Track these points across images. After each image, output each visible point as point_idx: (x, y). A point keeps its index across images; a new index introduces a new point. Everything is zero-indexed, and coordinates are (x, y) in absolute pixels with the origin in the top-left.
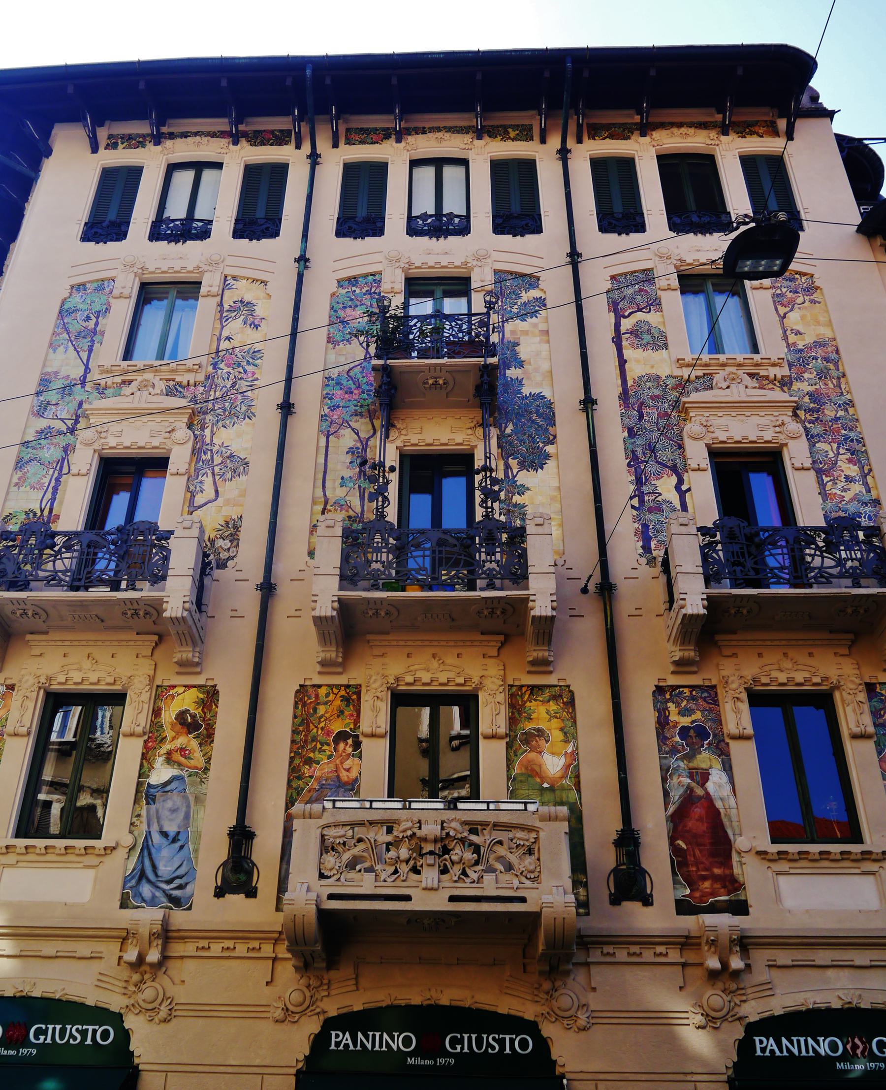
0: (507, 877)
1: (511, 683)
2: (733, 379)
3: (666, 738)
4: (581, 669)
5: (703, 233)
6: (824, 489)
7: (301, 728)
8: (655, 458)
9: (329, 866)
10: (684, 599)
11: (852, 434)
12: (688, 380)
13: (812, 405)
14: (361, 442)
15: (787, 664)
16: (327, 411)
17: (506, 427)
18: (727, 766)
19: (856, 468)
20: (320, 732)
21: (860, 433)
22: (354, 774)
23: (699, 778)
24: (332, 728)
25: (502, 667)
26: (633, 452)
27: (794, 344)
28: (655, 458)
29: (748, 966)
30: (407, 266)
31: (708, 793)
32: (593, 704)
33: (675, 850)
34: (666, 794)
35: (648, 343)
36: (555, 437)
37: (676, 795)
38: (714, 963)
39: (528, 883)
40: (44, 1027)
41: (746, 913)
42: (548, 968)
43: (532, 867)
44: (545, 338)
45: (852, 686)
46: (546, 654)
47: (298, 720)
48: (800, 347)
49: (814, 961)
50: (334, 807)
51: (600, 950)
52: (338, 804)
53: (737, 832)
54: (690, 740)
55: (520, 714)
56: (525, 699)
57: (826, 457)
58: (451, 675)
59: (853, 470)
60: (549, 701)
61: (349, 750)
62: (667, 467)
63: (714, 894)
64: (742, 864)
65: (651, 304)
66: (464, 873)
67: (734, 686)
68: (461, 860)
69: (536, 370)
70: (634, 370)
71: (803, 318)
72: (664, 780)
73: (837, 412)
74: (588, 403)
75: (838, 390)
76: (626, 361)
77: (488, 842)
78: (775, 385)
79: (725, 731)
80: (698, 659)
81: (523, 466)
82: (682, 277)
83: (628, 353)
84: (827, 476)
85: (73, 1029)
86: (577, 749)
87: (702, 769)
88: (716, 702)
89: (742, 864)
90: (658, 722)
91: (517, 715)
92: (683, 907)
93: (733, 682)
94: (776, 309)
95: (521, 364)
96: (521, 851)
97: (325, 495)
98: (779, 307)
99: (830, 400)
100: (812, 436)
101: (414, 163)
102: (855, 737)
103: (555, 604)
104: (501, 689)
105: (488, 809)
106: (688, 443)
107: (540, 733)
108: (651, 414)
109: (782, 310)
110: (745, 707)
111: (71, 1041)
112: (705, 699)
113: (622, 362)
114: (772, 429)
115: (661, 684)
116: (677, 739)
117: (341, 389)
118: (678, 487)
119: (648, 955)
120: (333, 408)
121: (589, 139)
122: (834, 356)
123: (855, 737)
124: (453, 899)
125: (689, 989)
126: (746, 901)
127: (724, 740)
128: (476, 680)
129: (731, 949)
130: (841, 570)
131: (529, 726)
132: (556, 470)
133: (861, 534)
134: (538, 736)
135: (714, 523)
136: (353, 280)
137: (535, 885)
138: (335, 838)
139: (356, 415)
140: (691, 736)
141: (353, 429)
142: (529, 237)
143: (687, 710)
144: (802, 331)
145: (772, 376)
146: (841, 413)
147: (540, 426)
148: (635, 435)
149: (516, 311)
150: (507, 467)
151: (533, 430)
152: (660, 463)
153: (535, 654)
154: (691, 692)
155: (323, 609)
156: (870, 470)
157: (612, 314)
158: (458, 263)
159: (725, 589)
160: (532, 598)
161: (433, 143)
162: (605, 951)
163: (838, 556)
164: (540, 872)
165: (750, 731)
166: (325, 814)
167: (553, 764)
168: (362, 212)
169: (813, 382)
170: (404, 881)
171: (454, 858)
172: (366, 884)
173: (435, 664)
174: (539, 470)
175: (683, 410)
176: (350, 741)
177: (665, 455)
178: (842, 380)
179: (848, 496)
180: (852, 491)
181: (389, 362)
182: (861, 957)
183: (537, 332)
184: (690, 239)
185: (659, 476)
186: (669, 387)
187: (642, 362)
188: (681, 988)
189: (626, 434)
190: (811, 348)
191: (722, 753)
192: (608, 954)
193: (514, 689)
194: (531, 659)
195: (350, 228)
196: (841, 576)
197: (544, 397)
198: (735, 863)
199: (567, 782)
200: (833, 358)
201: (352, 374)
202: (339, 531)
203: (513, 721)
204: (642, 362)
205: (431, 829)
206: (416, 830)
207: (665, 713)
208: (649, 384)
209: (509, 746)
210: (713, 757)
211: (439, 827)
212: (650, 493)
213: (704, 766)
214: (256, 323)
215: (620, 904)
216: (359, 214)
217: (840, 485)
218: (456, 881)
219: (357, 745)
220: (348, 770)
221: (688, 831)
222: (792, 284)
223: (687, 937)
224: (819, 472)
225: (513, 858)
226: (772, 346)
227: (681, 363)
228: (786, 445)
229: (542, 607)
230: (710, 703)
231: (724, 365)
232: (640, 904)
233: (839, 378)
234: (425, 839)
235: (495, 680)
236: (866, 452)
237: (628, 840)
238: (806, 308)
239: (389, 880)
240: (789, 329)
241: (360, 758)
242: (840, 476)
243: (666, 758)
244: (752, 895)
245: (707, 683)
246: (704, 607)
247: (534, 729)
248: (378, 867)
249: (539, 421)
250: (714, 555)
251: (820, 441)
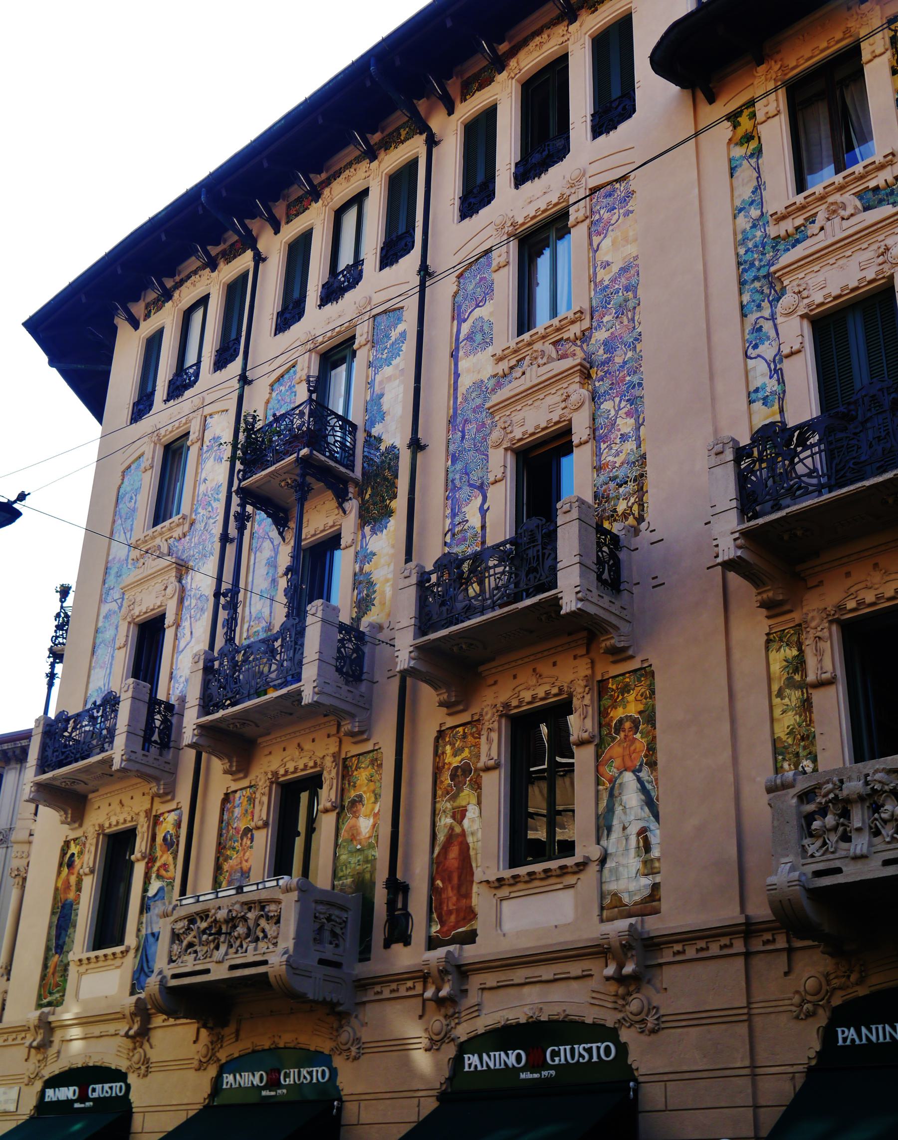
13: (605, 356)
23: (458, 816)
31: (463, 830)
37: (441, 838)
40: (556, 1048)
57: (607, 418)
73: (626, 354)
85: (579, 1048)
92: (432, 943)
99: (622, 343)
111: (581, 1060)
213: (464, 804)
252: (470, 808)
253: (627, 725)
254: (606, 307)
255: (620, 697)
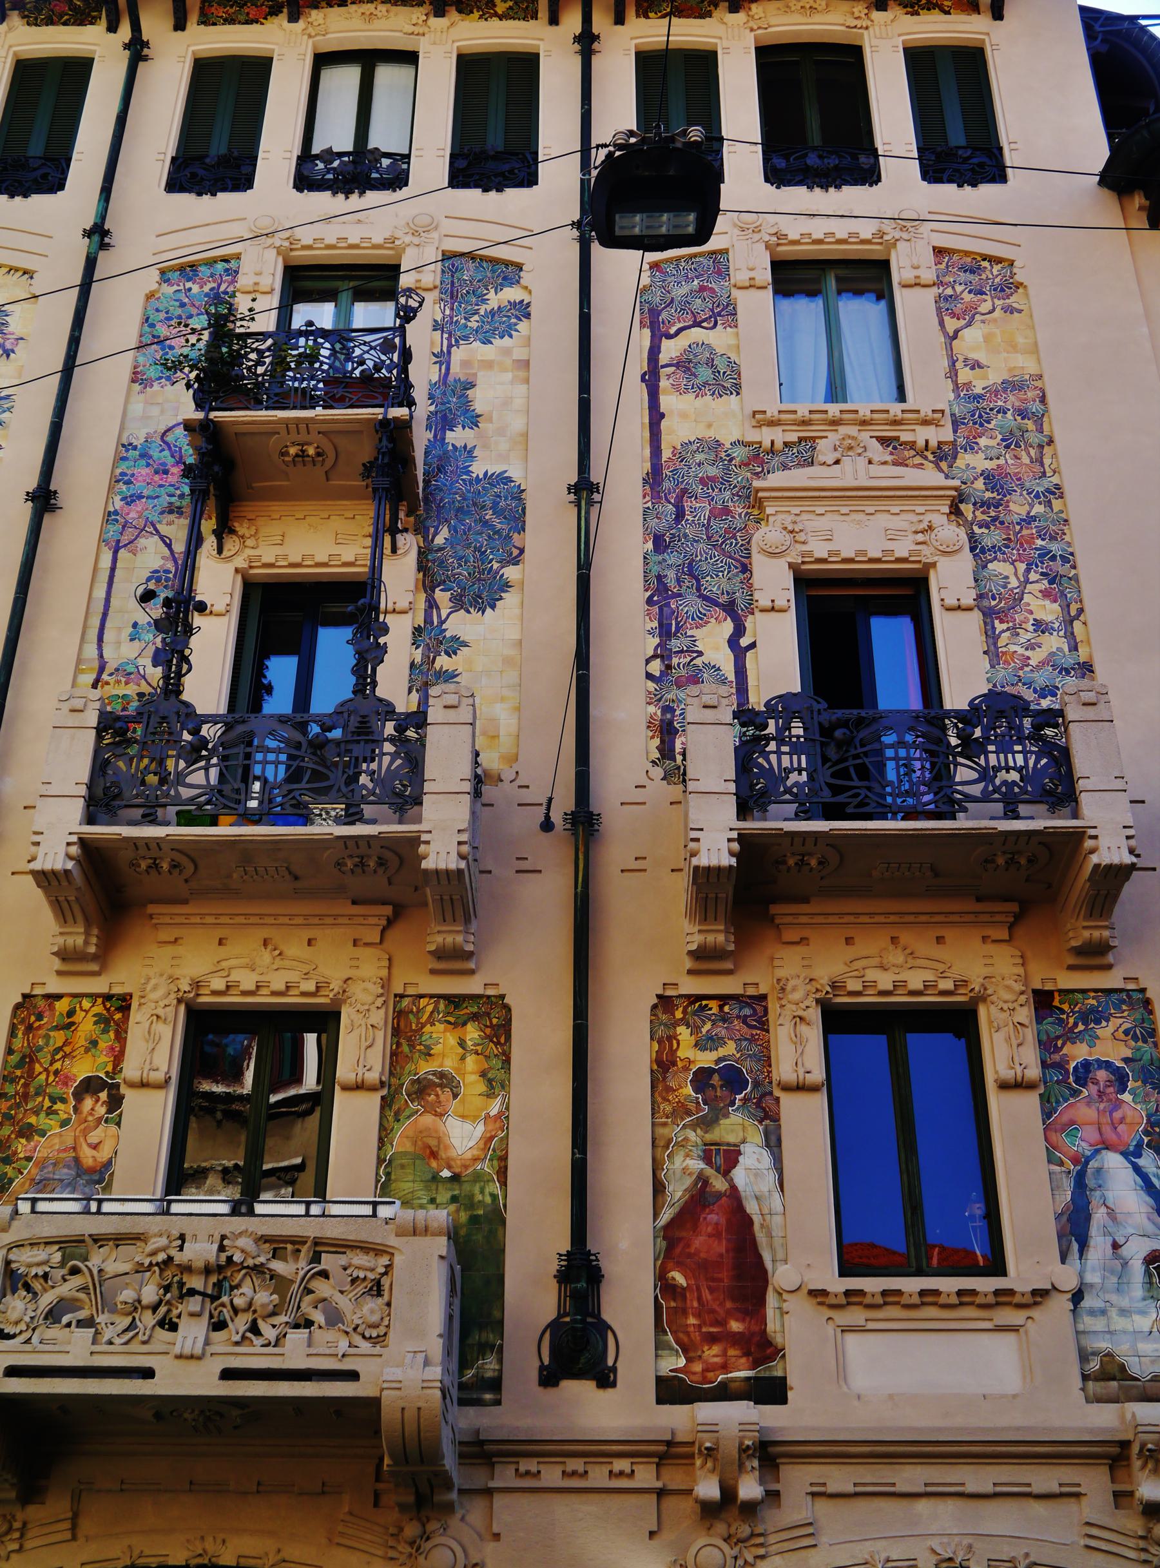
0: (330, 1335)
1: (400, 991)
2: (850, 448)
3: (669, 1090)
4: (526, 970)
5: (825, 187)
6: (995, 644)
7: (18, 1073)
8: (698, 590)
9: (14, 1316)
10: (697, 840)
11: (1054, 547)
12: (772, 451)
13: (988, 495)
14: (175, 560)
15: (896, 957)
16: (118, 504)
17: (436, 534)
18: (773, 1138)
19: (1056, 606)
20: (51, 1079)
21: (1069, 544)
22: (104, 1155)
23: (719, 1160)
24: (74, 1071)
25: (386, 963)
26: (659, 578)
27: (968, 385)
28: (698, 590)
29: (773, 1496)
30: (286, 244)
31: (734, 1188)
32: (541, 1031)
33: (665, 1287)
34: (659, 1188)
35: (706, 384)
36: (522, 551)
37: (677, 1191)
38: (709, 1489)
39: (365, 1346)
41: (783, 1401)
42: (411, 1499)
43: (375, 1318)
44: (522, 374)
45: (1009, 996)
46: (459, 939)
47: (14, 1059)
48: (978, 390)
49: (894, 1485)
50: (33, 1211)
51: (513, 1467)
52: (42, 1206)
53: (780, 1255)
54: (710, 1093)
55: (412, 1046)
56: (423, 1020)
57: (1005, 587)
58: (293, 977)
59: (1049, 611)
60: (464, 1024)
61: (101, 1110)
62: (717, 604)
63: (725, 1368)
64: (783, 1313)
65: (719, 314)
66: (255, 1329)
67: (797, 996)
68: (250, 1304)
69: (501, 431)
70: (675, 432)
71: (987, 338)
72: (656, 1166)
73: (1032, 506)
74: (585, 490)
75: (1037, 468)
76: (663, 416)
77: (301, 1273)
78: (926, 458)
79: (775, 1077)
80: (732, 947)
81: (459, 603)
82: (779, 267)
83: (667, 401)
84: (1002, 622)
86: (507, 1109)
87: (728, 1144)
88: (764, 1026)
89: (783, 1313)
90: (659, 1061)
91: (406, 1049)
92: (671, 1391)
93: (794, 989)
94: (942, 323)
95: (474, 421)
96: (360, 1289)
97: (101, 656)
98: (947, 319)
99: (1022, 486)
100: (983, 551)
101: (323, 60)
102: (1004, 1086)
103: (465, 849)
104: (380, 1001)
105: (307, 1214)
106: (759, 562)
107: (446, 1081)
108: (699, 509)
109: (951, 324)
110: (814, 1035)
112: (744, 1020)
113: (656, 417)
114: (911, 537)
115: (669, 993)
116: (689, 1090)
117: (148, 465)
118: (733, 642)
119: (598, 1476)
120: (129, 500)
121: (638, 16)
122: (1036, 407)
123: (1004, 1086)
124: (228, 1374)
125: (667, 1536)
126: (785, 1378)
127: (771, 1093)
128: (336, 985)
129: (741, 1466)
130: (986, 787)
131: (425, 1068)
132: (517, 611)
133: (1027, 722)
134: (442, 1086)
135: (767, 704)
136: (188, 270)
137: (377, 1350)
138: (30, 1266)
139: (171, 512)
140: (713, 1086)
141: (162, 538)
142: (510, 192)
143: (711, 1038)
144: (983, 361)
145: (921, 443)
146: (1039, 509)
147: (498, 532)
148: (667, 547)
149: (474, 325)
150: (432, 604)
151: (483, 539)
152: (705, 598)
153: (439, 939)
154: (721, 1007)
155: (50, 858)
156: (1081, 611)
157: (647, 332)
158: (378, 239)
159: (781, 820)
160: (424, 837)
161: (357, 23)
162: (522, 1469)
163: (982, 762)
164: (388, 1326)
165: (818, 1075)
166: (15, 1224)
167: (462, 1136)
168: (218, 147)
169: (994, 453)
170: (144, 1343)
171: (239, 1302)
172: (74, 1347)
173: (266, 956)
174: (488, 610)
175: (755, 502)
176: (103, 1095)
177: (714, 586)
178: (1046, 449)
179: (1036, 657)
180: (1044, 647)
181: (212, 415)
182: (978, 1478)
183: (508, 362)
184: (798, 197)
185: (701, 620)
186: (736, 462)
187: (689, 417)
188: (652, 1534)
189: (650, 545)
190: (996, 393)
191: (767, 1116)
192: (528, 1473)
193: (405, 1002)
194: (433, 948)
195: (194, 175)
196: (985, 798)
197: (509, 480)
198: (770, 1312)
199: (487, 1167)
200: (1035, 413)
201: (169, 438)
202: (92, 719)
203: (396, 1059)
204: (689, 417)
205: (200, 1251)
206: (173, 1252)
207: (671, 1045)
208: (699, 457)
209: (386, 1103)
210: (749, 1122)
211: (215, 1246)
212: (682, 651)
213: (732, 1139)
214: (8, 346)
215: (556, 1384)
216: (213, 152)
217: (1024, 637)
218: (237, 1344)
219: (115, 1102)
220: (95, 1147)
221: (690, 1255)
222: (974, 278)
223: (669, 1443)
224: (989, 615)
225: (343, 1303)
226: (929, 391)
227: (760, 419)
228: (934, 565)
229: (441, 854)
230: (754, 1027)
231: (835, 423)
232: (590, 1385)
233: (1041, 447)
234: (187, 1269)
235: (370, 986)
236: (1076, 578)
237: (581, 1273)
238: (995, 320)
239: (117, 1341)
240: (961, 358)
241: (118, 1124)
242: (1026, 621)
243: (665, 1124)
244: (794, 1368)
245: (751, 991)
246: (732, 854)
247: (434, 1073)
248: (101, 1319)
249: (498, 524)
250: (760, 760)
251: (995, 558)
252: (746, 1149)
253: (1102, 1075)
254: (981, 425)
255: (1081, 1027)
